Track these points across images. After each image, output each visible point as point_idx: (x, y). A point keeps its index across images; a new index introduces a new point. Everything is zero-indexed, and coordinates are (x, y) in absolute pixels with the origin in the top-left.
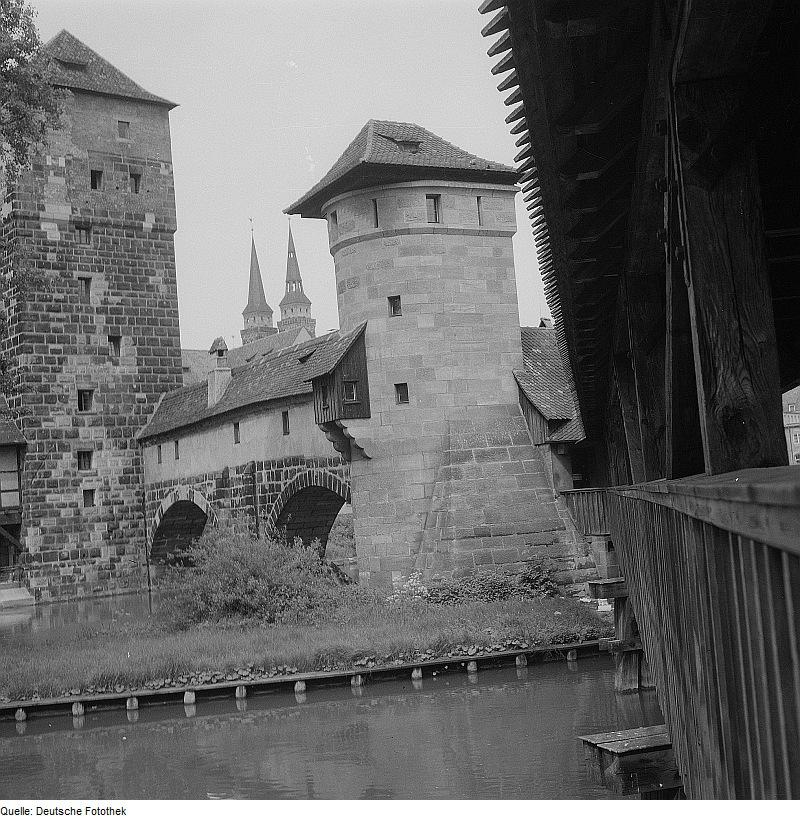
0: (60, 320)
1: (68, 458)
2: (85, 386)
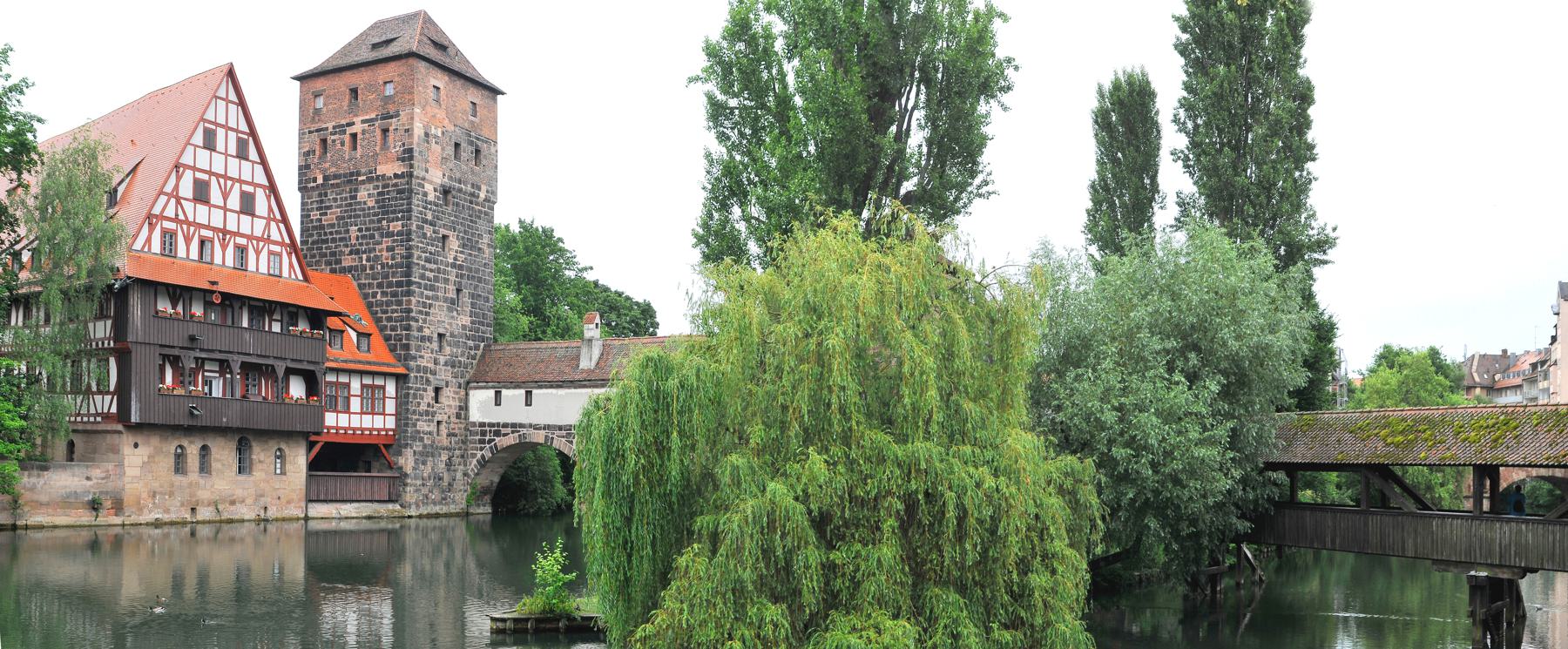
0: (431, 271)
1: (430, 390)
2: (441, 331)
